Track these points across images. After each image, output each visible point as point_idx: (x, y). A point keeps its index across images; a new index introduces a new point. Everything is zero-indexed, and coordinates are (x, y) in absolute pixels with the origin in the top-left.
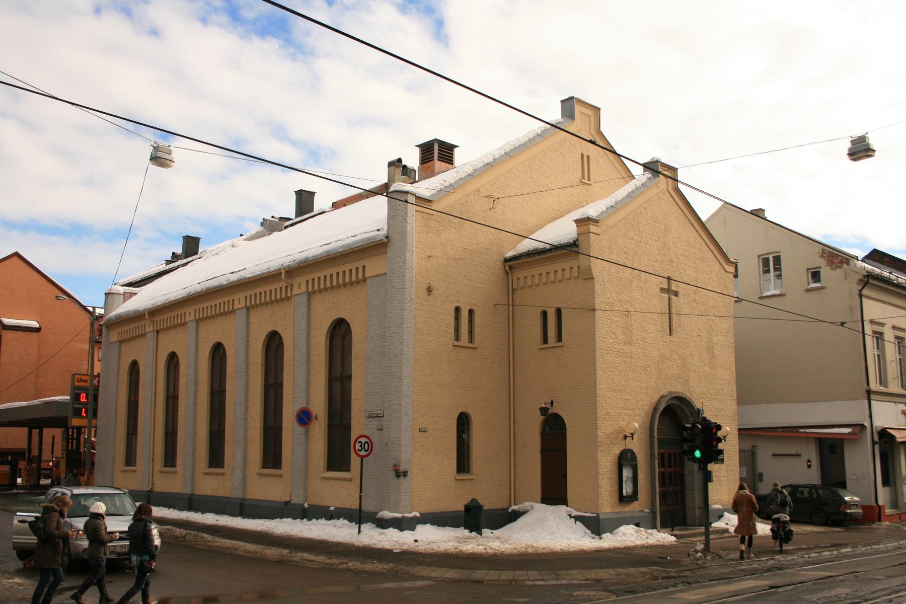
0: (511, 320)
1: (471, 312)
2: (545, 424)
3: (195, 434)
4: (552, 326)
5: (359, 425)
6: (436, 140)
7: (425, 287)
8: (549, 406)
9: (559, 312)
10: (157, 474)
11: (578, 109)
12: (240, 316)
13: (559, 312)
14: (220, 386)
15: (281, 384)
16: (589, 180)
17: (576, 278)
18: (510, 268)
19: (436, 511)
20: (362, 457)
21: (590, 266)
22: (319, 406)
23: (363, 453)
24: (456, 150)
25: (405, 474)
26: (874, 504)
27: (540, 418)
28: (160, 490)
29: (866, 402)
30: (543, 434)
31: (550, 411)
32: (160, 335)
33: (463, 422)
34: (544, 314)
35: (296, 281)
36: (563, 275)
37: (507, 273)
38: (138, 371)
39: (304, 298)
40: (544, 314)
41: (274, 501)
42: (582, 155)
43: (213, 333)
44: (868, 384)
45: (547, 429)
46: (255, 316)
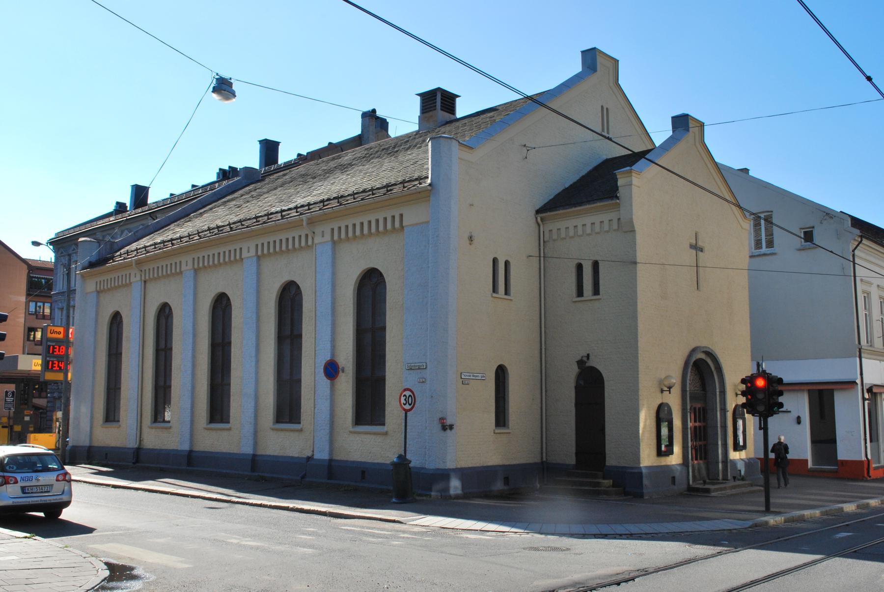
0: (543, 274)
1: (507, 264)
2: (579, 377)
3: (193, 387)
4: (588, 279)
5: (395, 377)
6: (439, 89)
7: (467, 236)
8: (585, 359)
9: (596, 265)
10: (146, 430)
11: (599, 59)
12: (250, 266)
13: (596, 265)
14: (223, 339)
15: (300, 336)
16: (608, 133)
17: (615, 230)
18: (542, 220)
19: (478, 465)
20: (406, 411)
21: (631, 219)
22: (346, 357)
23: (407, 407)
24: (457, 99)
25: (451, 427)
26: (864, 458)
27: (575, 370)
28: (151, 447)
29: (858, 359)
30: (578, 388)
31: (587, 365)
32: (147, 285)
33: (501, 373)
34: (580, 267)
35: (318, 230)
36: (610, 225)
37: (539, 225)
38: (121, 321)
39: (328, 248)
40: (580, 267)
41: (292, 457)
42: (602, 107)
43: (214, 284)
44: (859, 343)
45: (582, 383)
46: (268, 266)
